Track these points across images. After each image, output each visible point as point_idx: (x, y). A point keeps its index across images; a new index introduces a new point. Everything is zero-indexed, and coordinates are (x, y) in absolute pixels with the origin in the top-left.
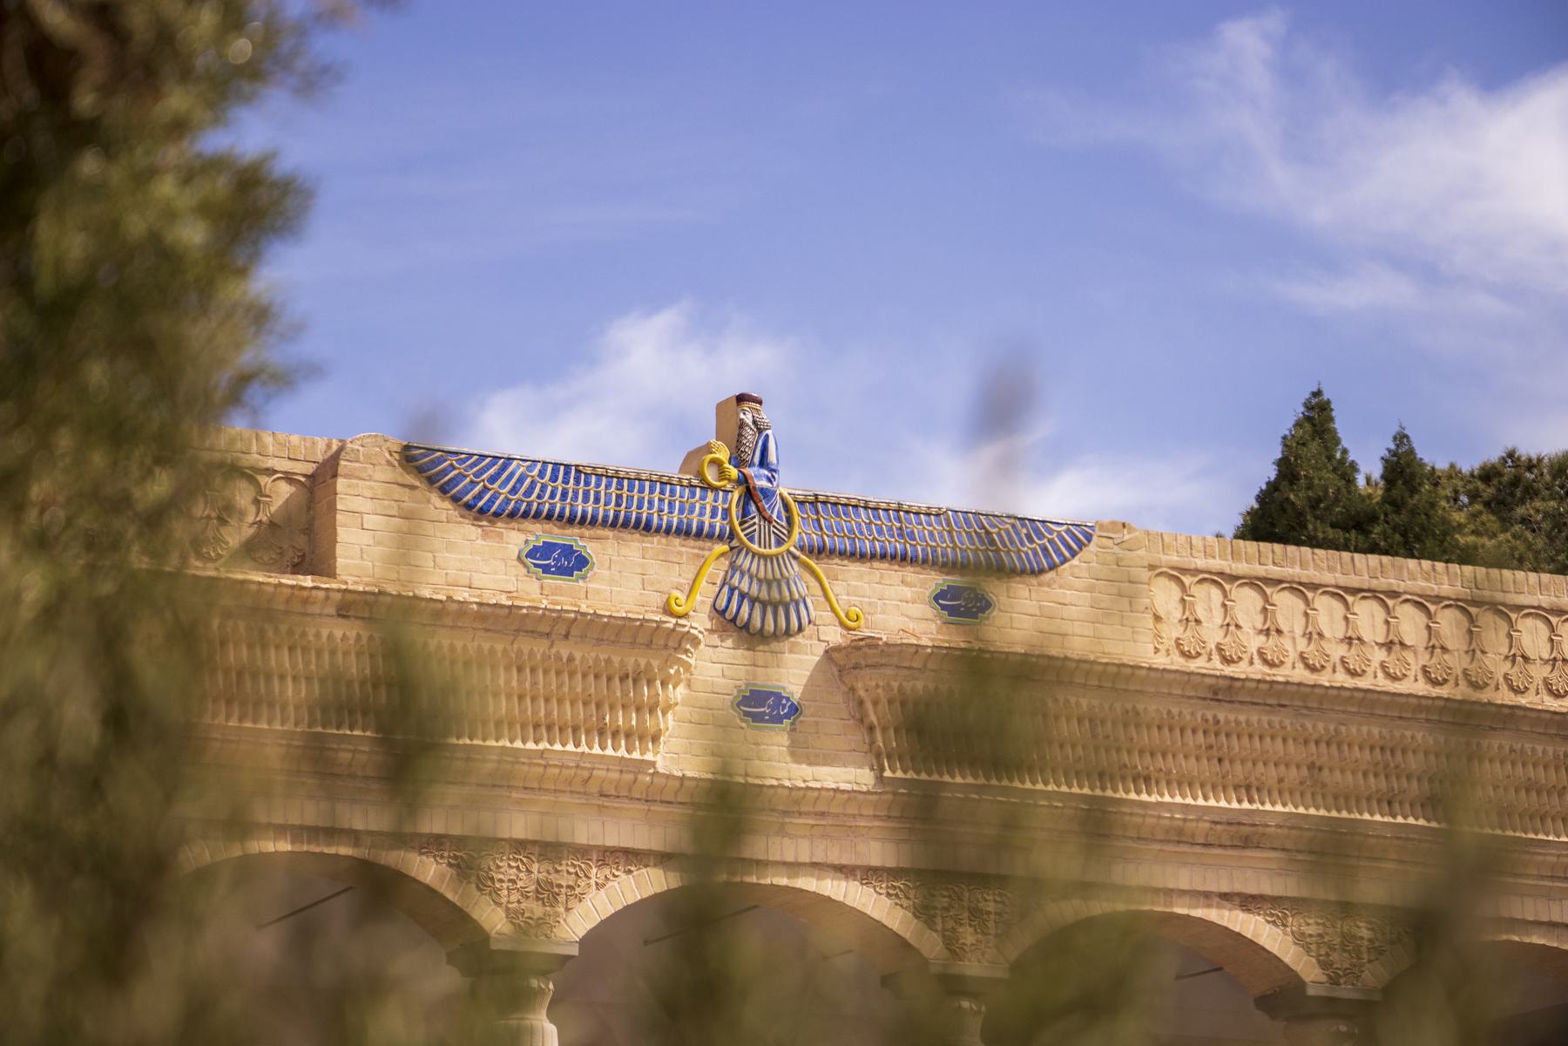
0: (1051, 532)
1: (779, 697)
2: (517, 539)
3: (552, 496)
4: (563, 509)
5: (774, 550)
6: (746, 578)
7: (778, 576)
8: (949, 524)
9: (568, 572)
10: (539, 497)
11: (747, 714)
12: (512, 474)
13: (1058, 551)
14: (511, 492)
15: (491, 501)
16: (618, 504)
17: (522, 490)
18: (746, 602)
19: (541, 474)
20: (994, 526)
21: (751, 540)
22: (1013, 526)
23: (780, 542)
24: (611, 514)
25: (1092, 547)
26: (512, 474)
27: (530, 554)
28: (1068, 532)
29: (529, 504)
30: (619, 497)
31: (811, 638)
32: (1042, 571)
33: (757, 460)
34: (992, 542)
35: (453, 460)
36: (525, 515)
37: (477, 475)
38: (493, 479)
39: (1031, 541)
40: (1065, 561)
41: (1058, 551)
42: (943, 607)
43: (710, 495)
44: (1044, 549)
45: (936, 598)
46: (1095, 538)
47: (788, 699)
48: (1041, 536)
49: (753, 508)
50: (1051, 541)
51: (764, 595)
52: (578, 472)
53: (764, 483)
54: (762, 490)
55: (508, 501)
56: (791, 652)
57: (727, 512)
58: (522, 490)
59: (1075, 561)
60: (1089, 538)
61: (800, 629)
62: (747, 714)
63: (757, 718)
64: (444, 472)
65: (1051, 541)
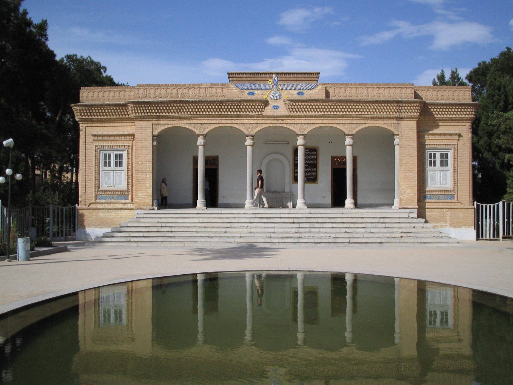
2: (247, 92)
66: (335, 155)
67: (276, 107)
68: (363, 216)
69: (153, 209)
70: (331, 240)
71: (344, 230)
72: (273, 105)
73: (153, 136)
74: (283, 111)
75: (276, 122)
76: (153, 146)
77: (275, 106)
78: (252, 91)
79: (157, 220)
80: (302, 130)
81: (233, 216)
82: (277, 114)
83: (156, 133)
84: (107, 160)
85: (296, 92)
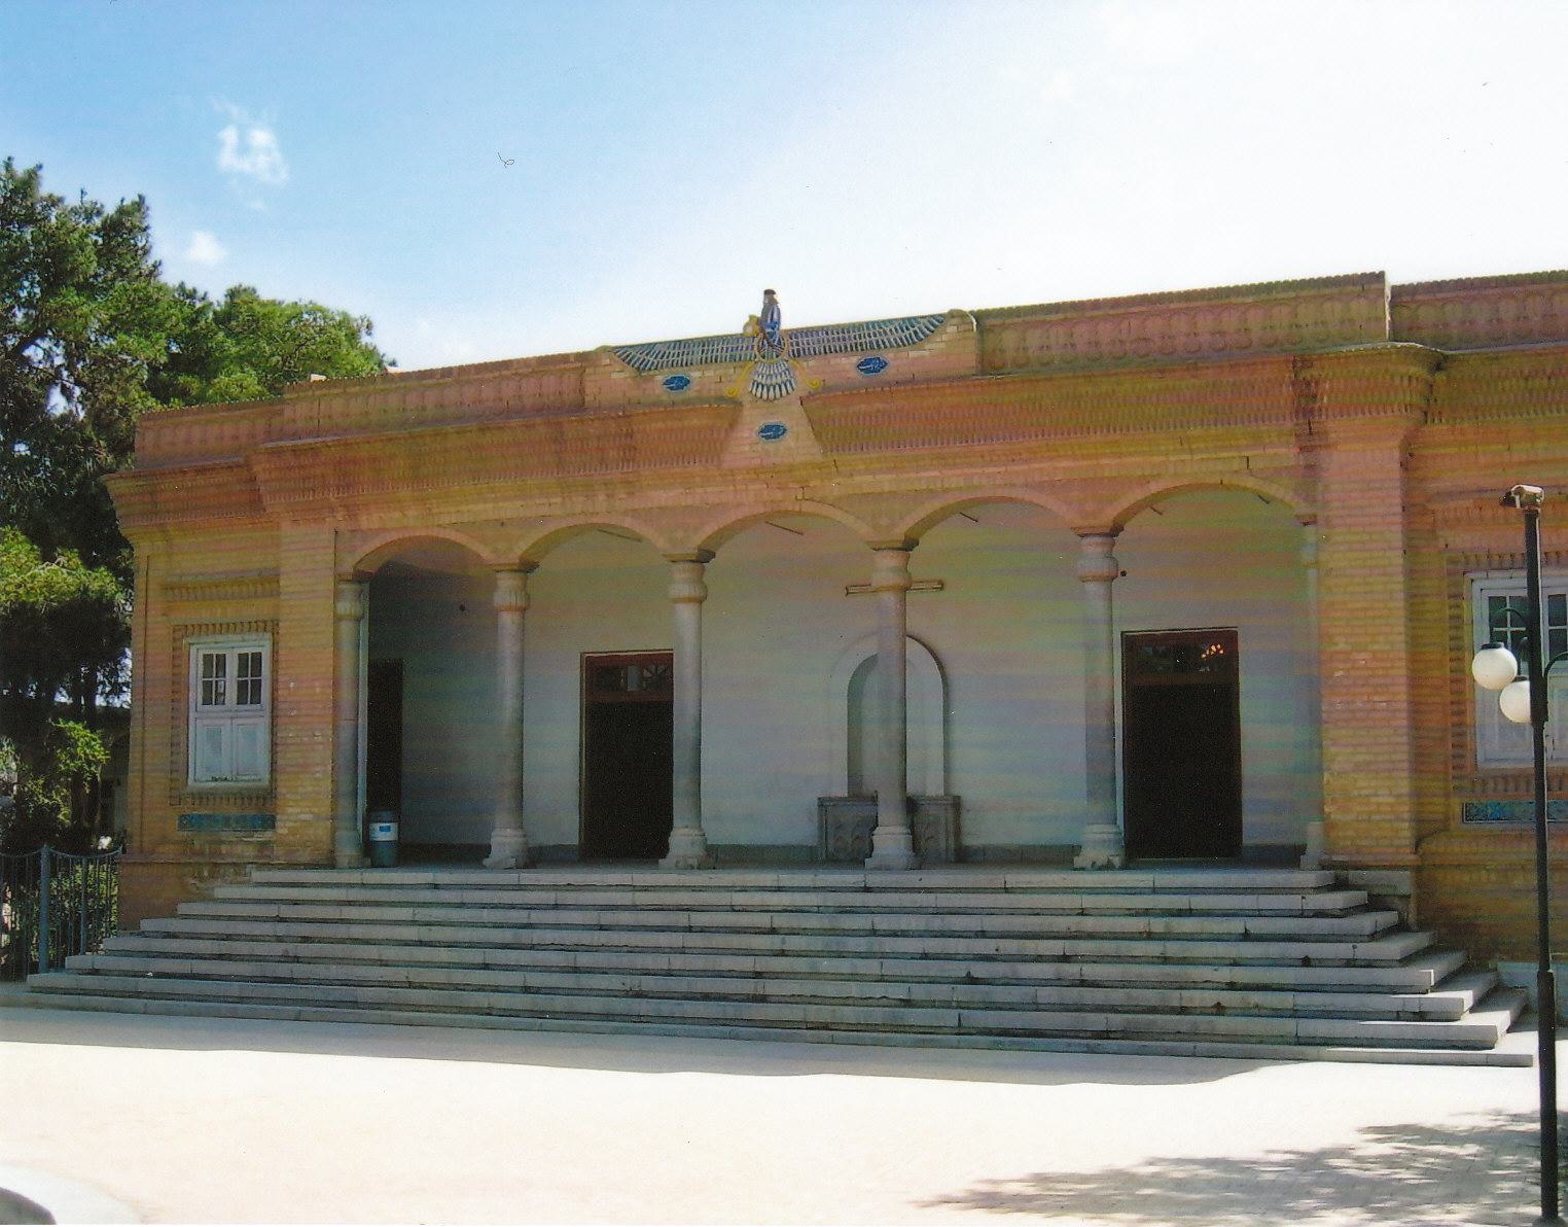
0: (919, 323)
17: (660, 356)
18: (760, 386)
21: (764, 357)
23: (777, 356)
35: (630, 351)
38: (647, 355)
39: (908, 329)
42: (862, 370)
44: (915, 332)
51: (769, 382)
53: (770, 330)
57: (753, 347)
58: (660, 356)
63: (768, 437)
64: (628, 356)
66: (1137, 627)
67: (773, 432)
68: (1089, 901)
69: (331, 864)
70: (878, 1015)
71: (958, 969)
72: (763, 423)
73: (339, 579)
74: (798, 445)
75: (779, 495)
76: (338, 619)
77: (768, 428)
78: (680, 372)
79: (272, 911)
80: (884, 522)
81: (549, 897)
82: (777, 460)
83: (348, 565)
84: (249, 678)
85: (855, 360)
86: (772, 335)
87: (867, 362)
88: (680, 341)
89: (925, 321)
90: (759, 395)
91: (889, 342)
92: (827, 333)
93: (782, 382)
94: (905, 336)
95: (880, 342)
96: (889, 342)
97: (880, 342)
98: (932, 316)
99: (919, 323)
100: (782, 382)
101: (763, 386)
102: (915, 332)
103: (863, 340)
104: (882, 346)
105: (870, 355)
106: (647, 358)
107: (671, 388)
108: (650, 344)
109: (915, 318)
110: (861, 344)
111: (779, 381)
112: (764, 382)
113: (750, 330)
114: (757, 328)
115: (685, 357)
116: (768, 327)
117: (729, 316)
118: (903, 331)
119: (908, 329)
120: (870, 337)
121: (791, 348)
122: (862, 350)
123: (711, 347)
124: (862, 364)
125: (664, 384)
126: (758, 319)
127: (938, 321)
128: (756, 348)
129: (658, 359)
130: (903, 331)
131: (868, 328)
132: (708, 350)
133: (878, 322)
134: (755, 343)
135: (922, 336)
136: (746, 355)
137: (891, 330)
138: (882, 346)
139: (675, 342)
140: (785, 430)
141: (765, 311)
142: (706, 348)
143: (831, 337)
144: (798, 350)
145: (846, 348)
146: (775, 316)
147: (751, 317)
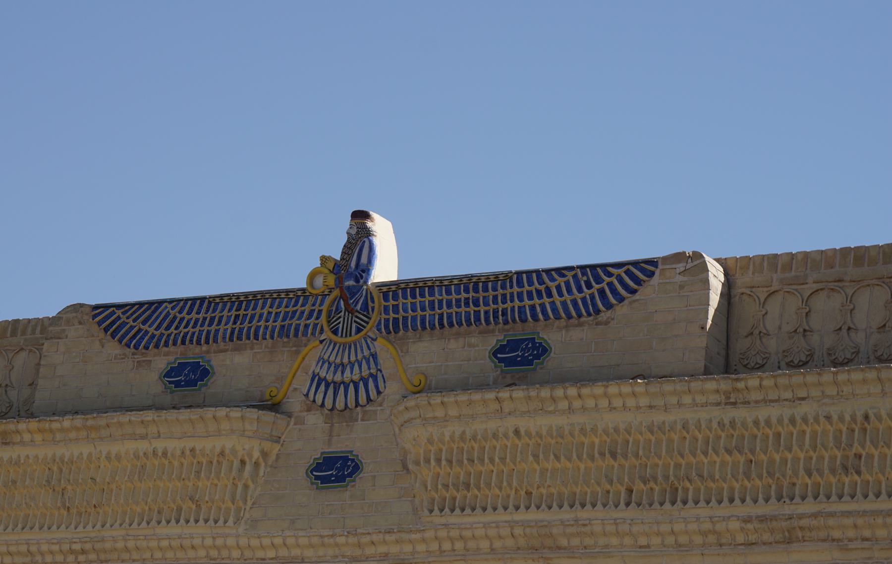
0: (610, 275)
1: (346, 459)
3: (186, 327)
4: (193, 333)
5: (354, 337)
6: (326, 365)
7: (353, 358)
8: (511, 287)
9: (191, 383)
10: (176, 328)
11: (317, 478)
12: (161, 313)
13: (614, 291)
14: (156, 329)
15: (142, 338)
16: (235, 323)
17: (164, 325)
19: (180, 312)
20: (553, 280)
21: (335, 332)
22: (575, 276)
23: (359, 331)
24: (229, 331)
25: (655, 280)
26: (161, 313)
27: (168, 375)
28: (628, 272)
29: (169, 335)
30: (237, 316)
31: (381, 405)
32: (598, 312)
33: (353, 264)
34: (550, 295)
35: (119, 312)
36: (166, 344)
37: (134, 321)
39: (589, 286)
40: (621, 300)
41: (614, 291)
42: (501, 360)
43: (311, 300)
44: (602, 292)
45: (495, 354)
46: (657, 272)
47: (353, 460)
48: (599, 280)
49: (342, 302)
50: (610, 284)
51: (338, 378)
52: (210, 303)
53: (351, 283)
54: (349, 288)
55: (153, 336)
56: (363, 420)
57: (320, 311)
58: (164, 325)
59: (637, 296)
60: (651, 274)
61: (369, 400)
62: (317, 478)
63: (325, 480)
64: (113, 323)
65: (610, 284)
67: (335, 470)
78: (193, 353)
86: (353, 292)
87: (513, 345)
88: (202, 299)
89: (621, 271)
90: (319, 401)
91: (554, 310)
92: (448, 292)
93: (362, 378)
94: (584, 300)
95: (538, 309)
96: (554, 310)
97: (538, 309)
98: (635, 264)
99: (610, 275)
100: (362, 378)
101: (327, 386)
102: (602, 292)
103: (509, 305)
104: (541, 316)
105: (518, 331)
106: (124, 318)
107: (177, 384)
108: (151, 303)
109: (604, 266)
110: (504, 313)
111: (356, 377)
112: (329, 378)
113: (319, 281)
114: (331, 280)
115: (206, 328)
116: (349, 275)
117: (285, 262)
118: (580, 290)
119: (589, 286)
120: (521, 300)
121: (384, 316)
122: (506, 322)
123: (250, 312)
124: (501, 349)
125: (164, 377)
126: (336, 264)
127: (643, 271)
128: (324, 314)
129: (162, 330)
130: (580, 290)
131: (520, 284)
132: (245, 316)
133: (537, 272)
134: (324, 308)
135: (613, 301)
136: (307, 326)
137: (558, 288)
138: (541, 316)
139: (194, 300)
140: (357, 468)
141: (348, 249)
142: (242, 312)
143: (454, 296)
144: (396, 320)
145: (477, 319)
146: (364, 260)
147: (324, 259)
